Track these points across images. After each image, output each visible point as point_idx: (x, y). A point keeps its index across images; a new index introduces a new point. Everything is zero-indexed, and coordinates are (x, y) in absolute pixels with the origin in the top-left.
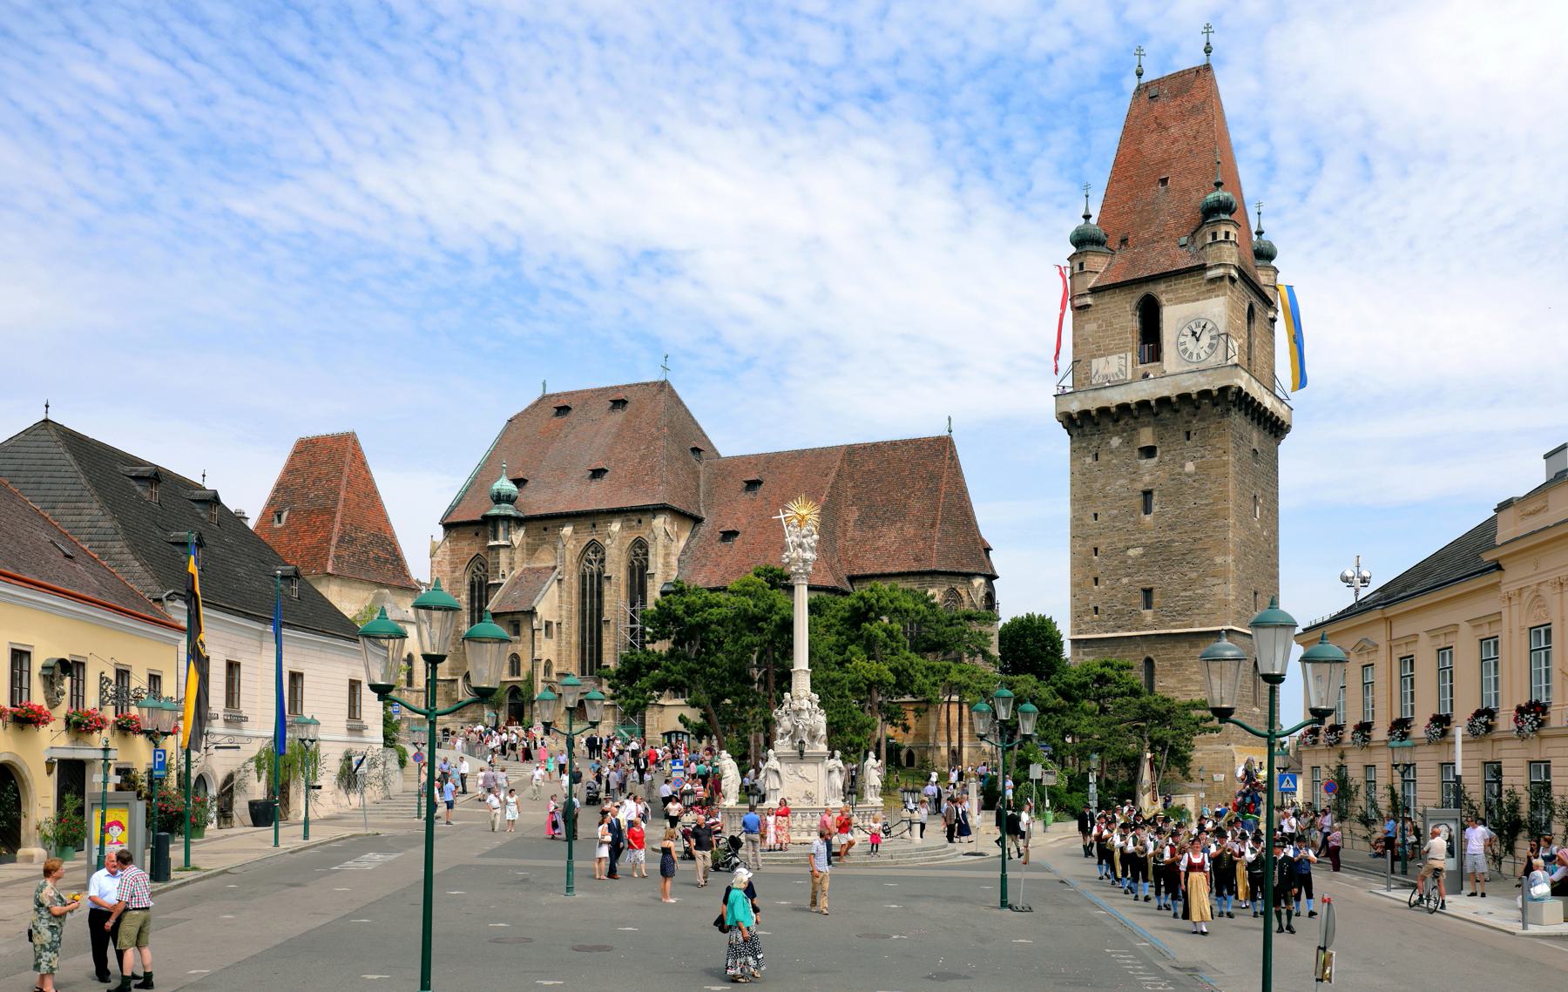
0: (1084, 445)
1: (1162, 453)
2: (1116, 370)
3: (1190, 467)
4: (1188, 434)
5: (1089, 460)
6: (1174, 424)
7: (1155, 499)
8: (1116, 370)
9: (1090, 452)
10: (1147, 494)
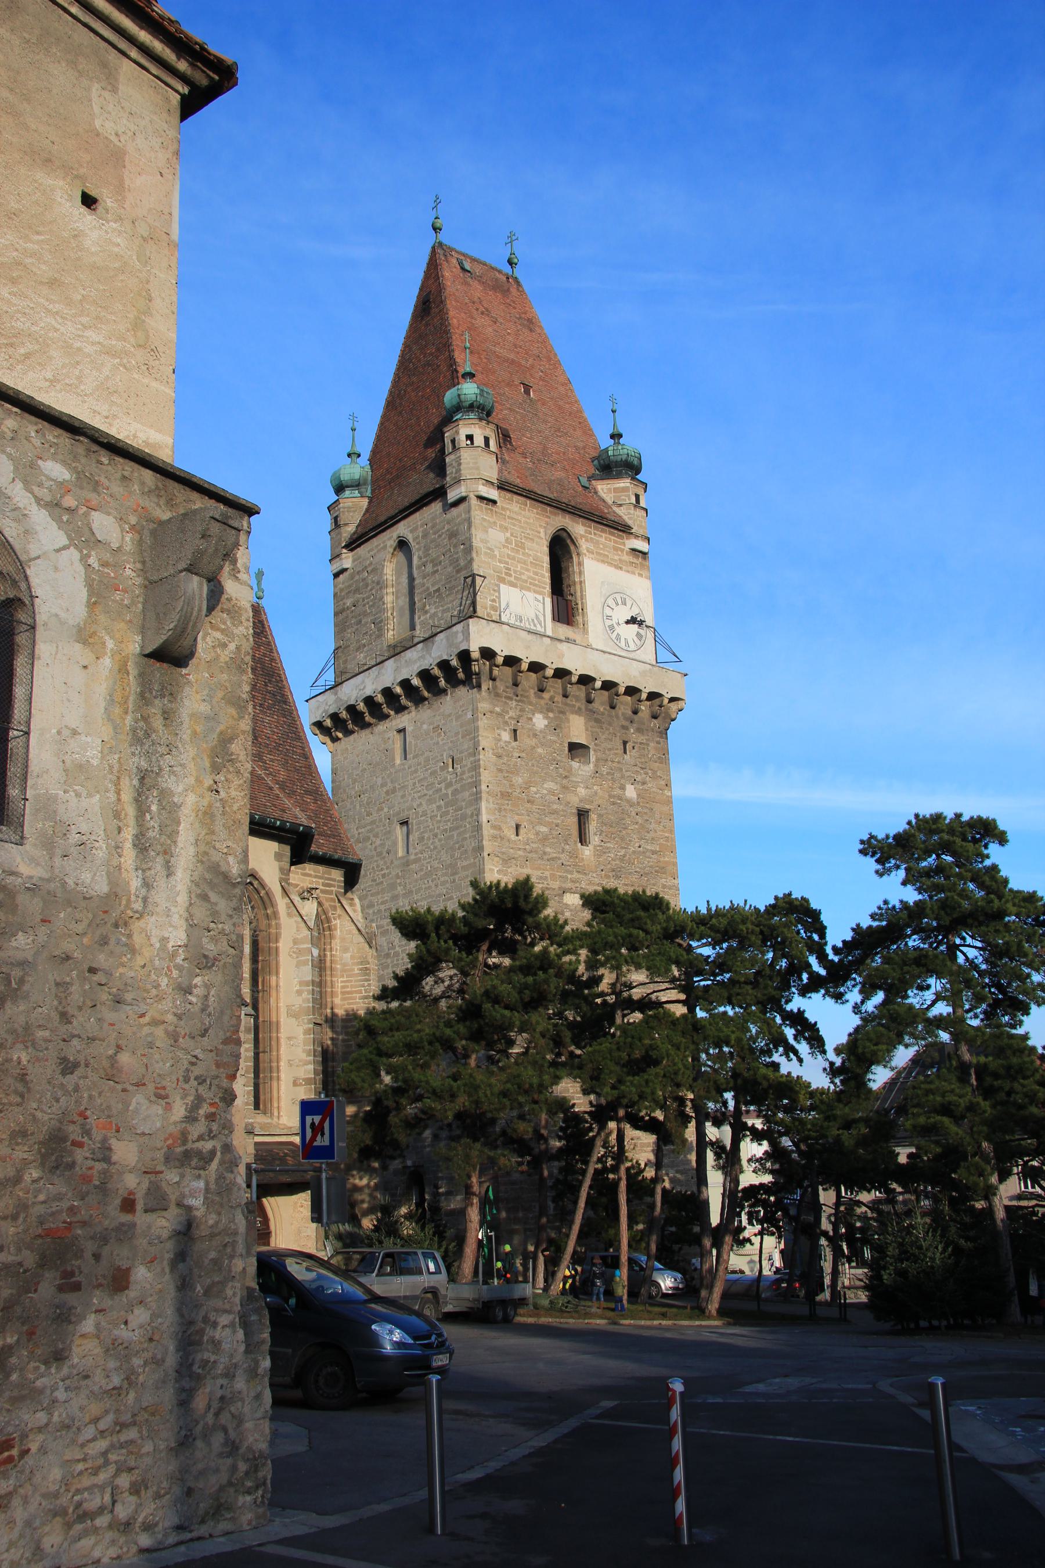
0: (498, 709)
1: (597, 760)
2: (532, 616)
3: (631, 792)
4: (625, 743)
5: (506, 736)
6: (610, 724)
7: (593, 826)
8: (532, 616)
9: (506, 723)
10: (582, 815)
